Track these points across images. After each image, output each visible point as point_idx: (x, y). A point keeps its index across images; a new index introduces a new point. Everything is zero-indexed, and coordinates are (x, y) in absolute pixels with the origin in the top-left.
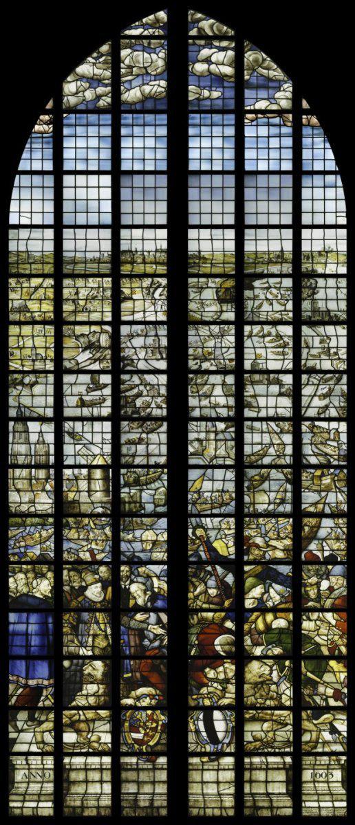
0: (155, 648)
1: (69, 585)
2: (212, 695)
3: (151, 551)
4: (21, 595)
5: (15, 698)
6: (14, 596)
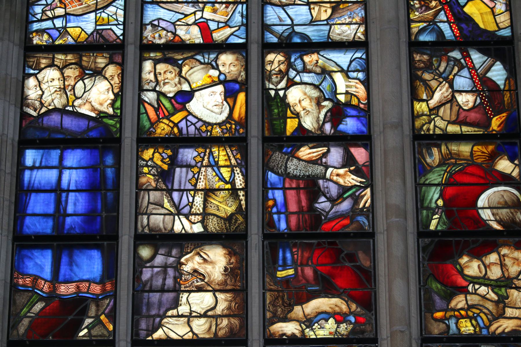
0: (342, 216)
1: (154, 90)
2: (478, 311)
3: (328, 22)
4: (49, 112)
5: (26, 322)
6: (35, 114)
